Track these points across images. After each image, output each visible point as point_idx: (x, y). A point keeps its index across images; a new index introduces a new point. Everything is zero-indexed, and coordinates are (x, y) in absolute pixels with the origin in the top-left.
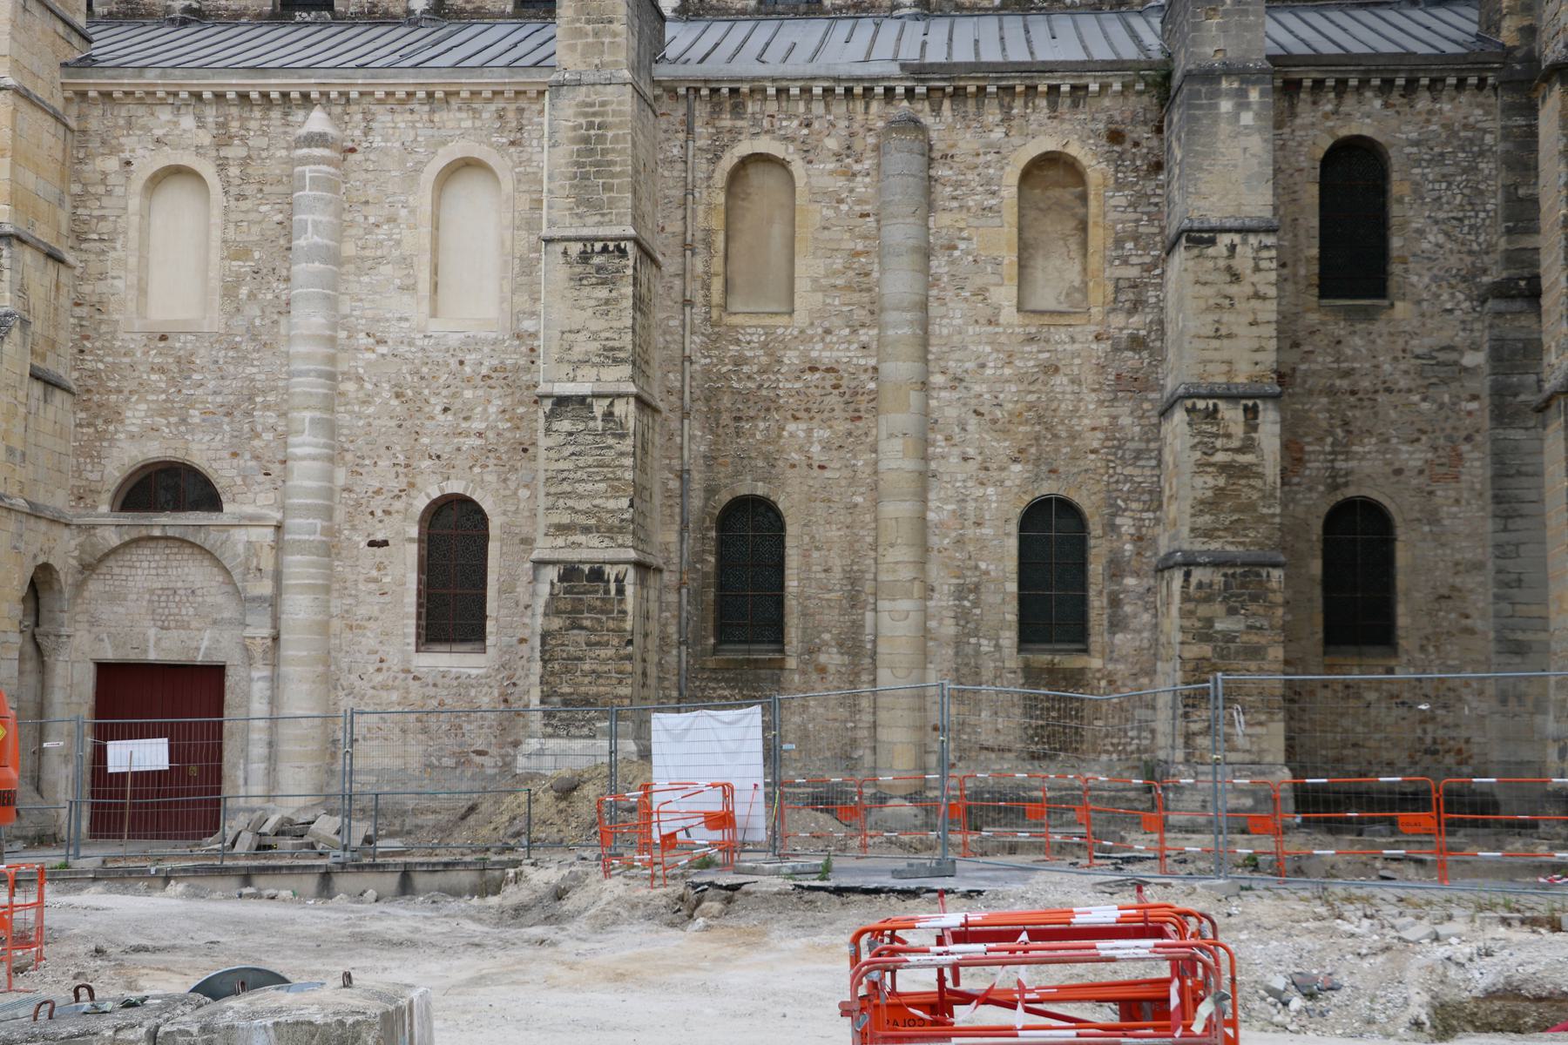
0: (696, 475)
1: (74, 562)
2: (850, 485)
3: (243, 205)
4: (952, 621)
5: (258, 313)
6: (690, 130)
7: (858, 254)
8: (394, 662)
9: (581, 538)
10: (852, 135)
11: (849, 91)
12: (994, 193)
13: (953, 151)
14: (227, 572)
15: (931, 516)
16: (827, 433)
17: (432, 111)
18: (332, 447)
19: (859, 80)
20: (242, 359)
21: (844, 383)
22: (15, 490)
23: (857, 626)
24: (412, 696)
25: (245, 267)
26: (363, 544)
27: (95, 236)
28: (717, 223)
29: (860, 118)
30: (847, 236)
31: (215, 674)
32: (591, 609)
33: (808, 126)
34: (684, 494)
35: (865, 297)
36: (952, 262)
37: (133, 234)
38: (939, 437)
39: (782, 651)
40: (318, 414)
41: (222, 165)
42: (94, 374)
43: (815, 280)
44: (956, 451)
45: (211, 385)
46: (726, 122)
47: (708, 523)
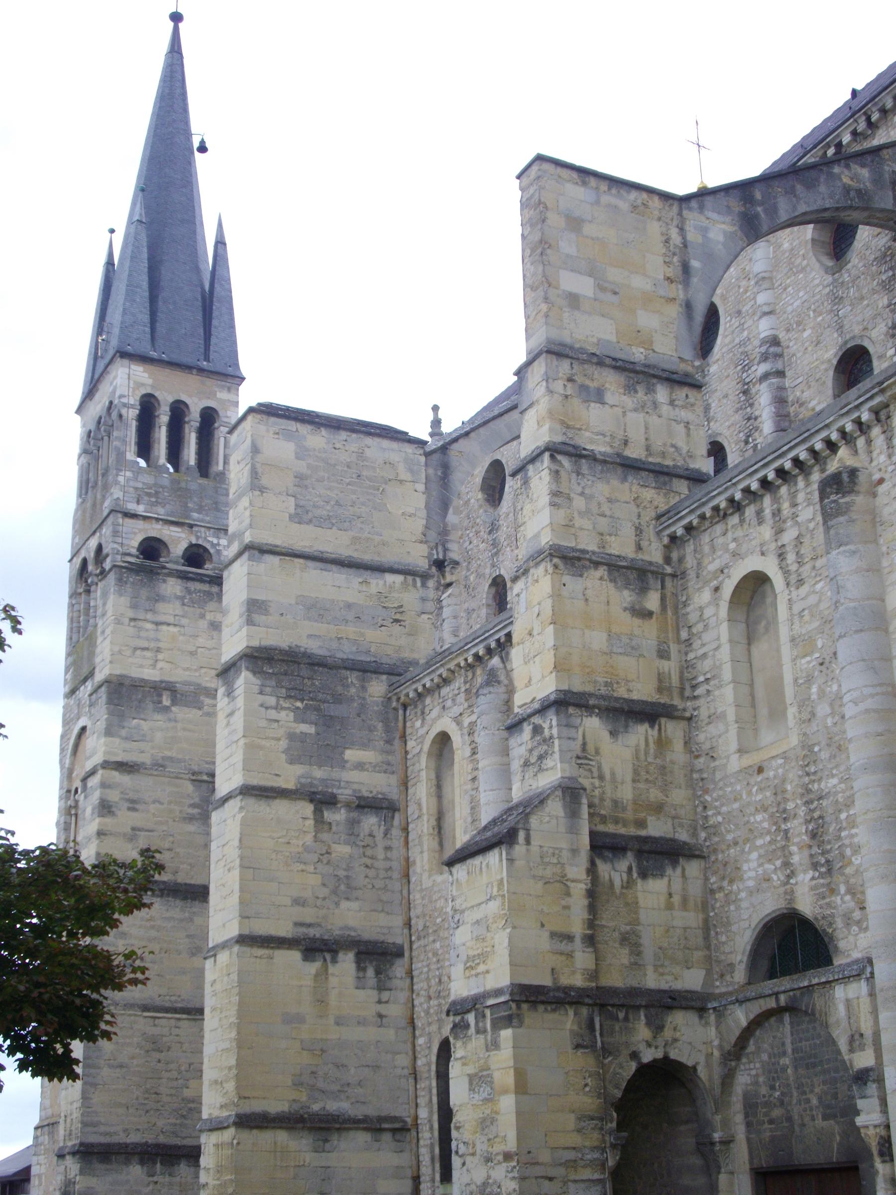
1: (716, 1053)
5: (828, 710)
27: (701, 679)
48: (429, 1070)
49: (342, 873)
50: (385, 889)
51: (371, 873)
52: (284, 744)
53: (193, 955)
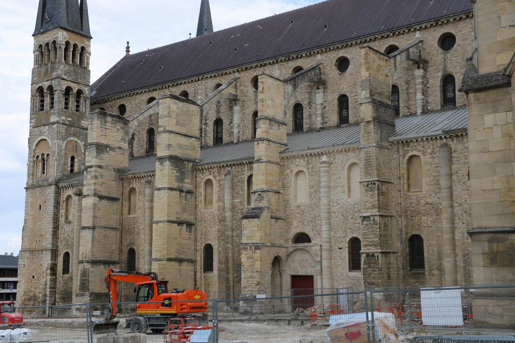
0: (403, 230)
2: (437, 231)
3: (313, 177)
4: (463, 263)
6: (398, 151)
7: (436, 176)
8: (345, 274)
9: (370, 247)
10: (434, 148)
11: (432, 138)
12: (467, 159)
13: (457, 150)
14: (312, 256)
15: (456, 237)
16: (431, 219)
17: (346, 153)
18: (331, 228)
19: (433, 136)
20: (313, 210)
21: (434, 207)
22: (268, 242)
23: (441, 264)
24: (349, 282)
25: (313, 190)
26: (337, 249)
28: (405, 172)
29: (435, 144)
30: (433, 172)
31: (311, 278)
32: (373, 263)
33: (424, 147)
34: (401, 234)
35: (438, 186)
36: (458, 176)
37: (293, 185)
38: (457, 218)
39: (424, 270)
40: (326, 221)
41: (308, 170)
42: (287, 215)
43: (427, 183)
44: (461, 221)
45: (308, 216)
46: (406, 148)
47: (406, 241)
48: (201, 250)
49: (184, 207)
50: (191, 210)
51: (189, 207)
52: (174, 178)
53: (114, 214)
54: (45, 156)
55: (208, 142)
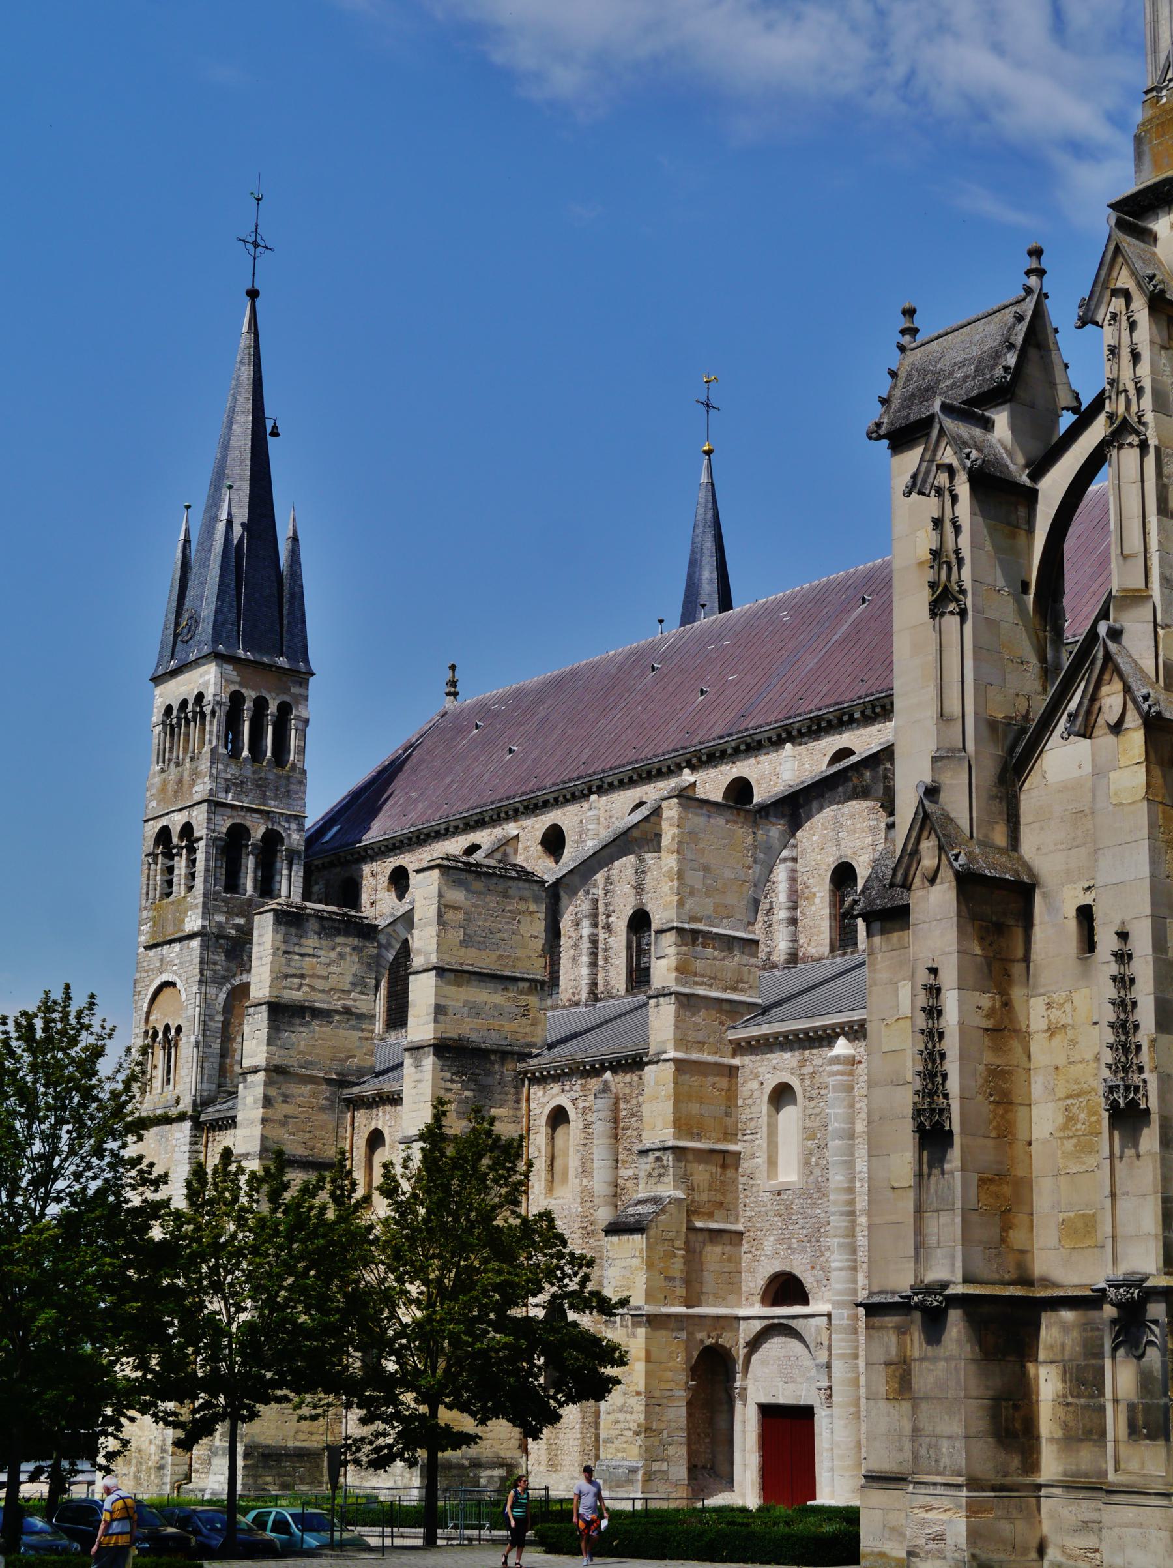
20: (814, 1205)
37: (765, 1129)
40: (842, 1240)
41: (802, 1080)
45: (801, 1221)
54: (173, 1032)
55: (612, 983)
